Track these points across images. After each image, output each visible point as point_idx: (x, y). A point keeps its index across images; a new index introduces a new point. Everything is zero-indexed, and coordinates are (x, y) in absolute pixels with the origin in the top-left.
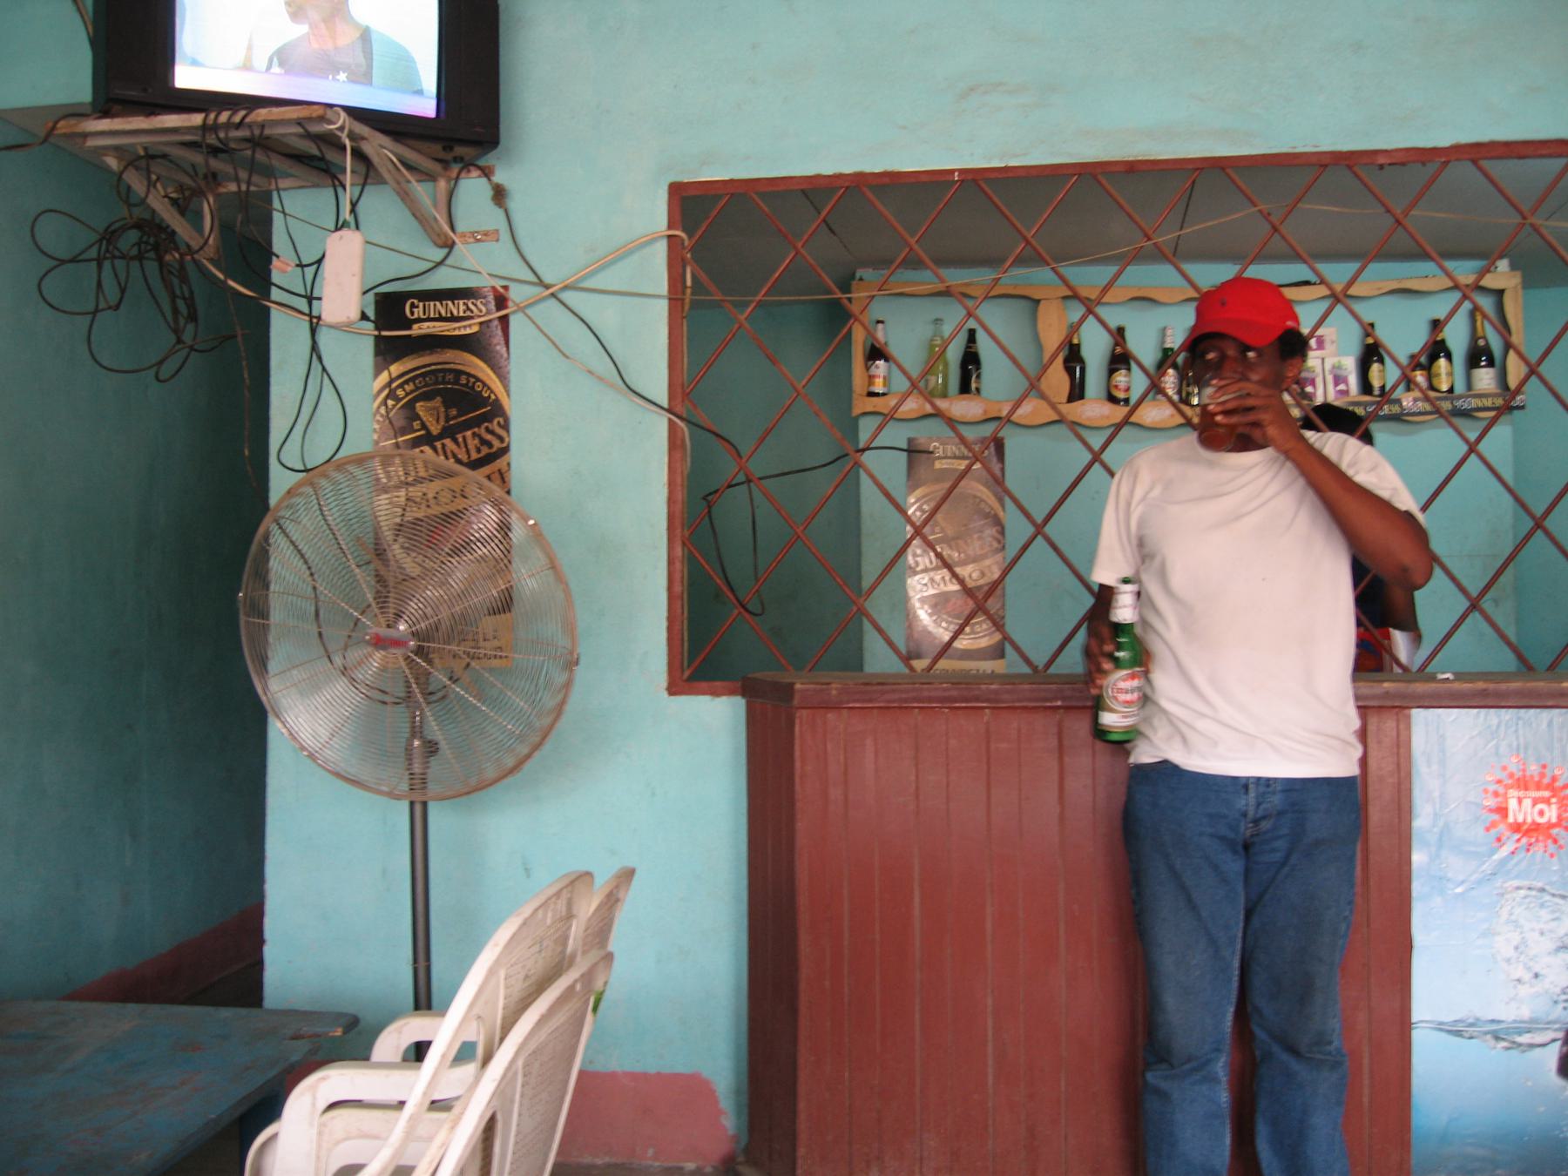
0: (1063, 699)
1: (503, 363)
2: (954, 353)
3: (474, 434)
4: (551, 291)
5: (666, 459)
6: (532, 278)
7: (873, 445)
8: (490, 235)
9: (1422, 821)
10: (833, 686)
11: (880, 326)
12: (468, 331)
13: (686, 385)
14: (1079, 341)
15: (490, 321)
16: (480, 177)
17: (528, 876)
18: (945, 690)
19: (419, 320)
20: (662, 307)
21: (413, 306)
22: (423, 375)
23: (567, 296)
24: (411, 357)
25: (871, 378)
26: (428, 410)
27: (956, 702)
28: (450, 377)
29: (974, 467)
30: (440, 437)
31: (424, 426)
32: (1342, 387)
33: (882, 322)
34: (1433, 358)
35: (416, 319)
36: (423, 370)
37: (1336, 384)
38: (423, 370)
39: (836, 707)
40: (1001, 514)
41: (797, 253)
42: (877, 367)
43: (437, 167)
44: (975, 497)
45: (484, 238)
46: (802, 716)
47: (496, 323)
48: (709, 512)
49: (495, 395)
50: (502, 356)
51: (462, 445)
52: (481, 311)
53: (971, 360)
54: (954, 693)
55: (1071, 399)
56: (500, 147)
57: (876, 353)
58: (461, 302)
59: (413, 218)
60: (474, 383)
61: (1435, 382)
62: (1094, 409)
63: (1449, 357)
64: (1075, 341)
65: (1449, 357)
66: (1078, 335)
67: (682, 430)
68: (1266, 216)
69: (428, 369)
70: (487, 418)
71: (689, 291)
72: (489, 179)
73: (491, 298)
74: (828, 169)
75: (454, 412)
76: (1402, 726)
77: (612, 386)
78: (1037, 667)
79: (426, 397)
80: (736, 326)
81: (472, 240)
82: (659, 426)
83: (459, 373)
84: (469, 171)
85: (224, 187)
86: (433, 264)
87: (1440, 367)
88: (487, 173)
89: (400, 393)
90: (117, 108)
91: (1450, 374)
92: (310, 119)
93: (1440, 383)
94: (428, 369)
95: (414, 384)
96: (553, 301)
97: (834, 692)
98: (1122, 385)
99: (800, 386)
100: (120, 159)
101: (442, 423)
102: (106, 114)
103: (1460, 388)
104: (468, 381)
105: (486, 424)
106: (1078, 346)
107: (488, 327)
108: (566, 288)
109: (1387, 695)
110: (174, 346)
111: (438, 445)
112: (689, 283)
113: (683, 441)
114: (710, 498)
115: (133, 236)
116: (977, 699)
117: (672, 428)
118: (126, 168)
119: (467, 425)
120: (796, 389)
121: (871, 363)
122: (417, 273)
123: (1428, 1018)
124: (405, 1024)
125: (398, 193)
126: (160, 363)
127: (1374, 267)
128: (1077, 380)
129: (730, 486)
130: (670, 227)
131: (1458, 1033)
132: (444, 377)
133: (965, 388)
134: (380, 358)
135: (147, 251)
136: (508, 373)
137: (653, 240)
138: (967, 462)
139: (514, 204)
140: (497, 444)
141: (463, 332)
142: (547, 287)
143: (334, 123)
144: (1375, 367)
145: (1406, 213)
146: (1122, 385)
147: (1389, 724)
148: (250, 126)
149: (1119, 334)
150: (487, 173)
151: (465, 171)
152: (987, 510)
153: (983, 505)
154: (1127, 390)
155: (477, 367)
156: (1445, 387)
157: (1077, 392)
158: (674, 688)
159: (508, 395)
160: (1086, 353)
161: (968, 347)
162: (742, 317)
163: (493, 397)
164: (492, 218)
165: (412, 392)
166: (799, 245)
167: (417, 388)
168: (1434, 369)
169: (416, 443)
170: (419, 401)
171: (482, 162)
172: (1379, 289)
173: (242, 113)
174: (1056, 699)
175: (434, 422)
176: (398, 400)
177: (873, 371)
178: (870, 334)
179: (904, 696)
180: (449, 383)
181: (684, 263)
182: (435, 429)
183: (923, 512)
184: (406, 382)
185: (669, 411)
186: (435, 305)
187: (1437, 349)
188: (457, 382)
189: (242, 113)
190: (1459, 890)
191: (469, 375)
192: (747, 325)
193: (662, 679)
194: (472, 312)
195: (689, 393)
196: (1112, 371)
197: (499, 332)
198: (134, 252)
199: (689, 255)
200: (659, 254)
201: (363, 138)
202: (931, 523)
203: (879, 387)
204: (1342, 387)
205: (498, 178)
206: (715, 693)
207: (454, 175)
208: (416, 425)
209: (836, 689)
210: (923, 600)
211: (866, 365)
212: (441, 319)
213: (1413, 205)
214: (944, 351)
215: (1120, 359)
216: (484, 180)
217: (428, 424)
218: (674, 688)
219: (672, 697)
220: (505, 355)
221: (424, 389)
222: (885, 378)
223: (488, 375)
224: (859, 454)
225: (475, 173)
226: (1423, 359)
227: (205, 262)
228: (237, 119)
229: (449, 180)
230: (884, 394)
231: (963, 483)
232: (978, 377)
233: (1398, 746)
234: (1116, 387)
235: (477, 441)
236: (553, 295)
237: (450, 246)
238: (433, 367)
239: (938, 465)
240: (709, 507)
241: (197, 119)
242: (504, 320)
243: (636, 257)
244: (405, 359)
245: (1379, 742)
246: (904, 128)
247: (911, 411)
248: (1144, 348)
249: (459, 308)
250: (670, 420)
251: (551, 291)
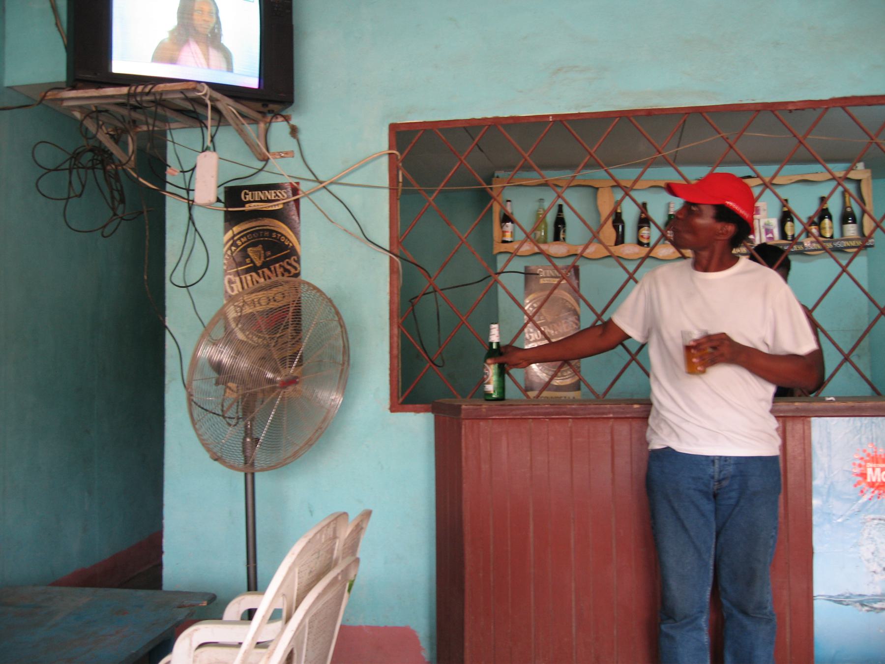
0: (613, 413)
1: (297, 226)
2: (551, 218)
3: (281, 266)
4: (323, 185)
5: (388, 279)
6: (313, 178)
7: (505, 271)
8: (289, 154)
9: (818, 481)
10: (484, 406)
11: (509, 203)
12: (277, 208)
13: (399, 237)
14: (621, 210)
15: (289, 202)
16: (283, 121)
17: (312, 515)
18: (547, 408)
19: (249, 202)
20: (386, 193)
21: (246, 194)
22: (252, 233)
23: (333, 188)
24: (246, 222)
25: (504, 232)
26: (254, 252)
27: (553, 415)
28: (267, 234)
29: (562, 282)
30: (262, 267)
31: (252, 261)
32: (770, 235)
34: (821, 219)
35: (247, 201)
36: (252, 230)
37: (767, 233)
38: (252, 230)
39: (485, 419)
40: (578, 309)
41: (461, 163)
42: (507, 226)
43: (259, 116)
44: (563, 299)
45: (286, 155)
46: (466, 424)
47: (292, 203)
48: (413, 310)
49: (292, 244)
50: (295, 222)
51: (274, 272)
52: (284, 196)
53: (560, 222)
54: (552, 410)
55: (617, 244)
56: (294, 104)
57: (506, 218)
58: (273, 191)
59: (246, 145)
60: (280, 237)
61: (823, 232)
62: (629, 249)
64: (619, 211)
66: (621, 208)
67: (397, 263)
68: (726, 139)
69: (254, 229)
70: (288, 256)
71: (401, 184)
72: (288, 123)
73: (289, 189)
74: (478, 115)
75: (269, 253)
76: (806, 427)
77: (357, 238)
78: (598, 395)
79: (254, 245)
80: (427, 204)
81: (278, 157)
82: (384, 261)
83: (272, 231)
84: (277, 118)
85: (140, 128)
86: (255, 171)
87: (825, 224)
88: (287, 119)
89: (239, 243)
90: (80, 85)
92: (187, 90)
93: (826, 232)
94: (254, 229)
95: (247, 237)
96: (324, 190)
97: (484, 410)
98: (646, 236)
99: (463, 237)
100: (81, 113)
101: (262, 259)
102: (74, 88)
104: (277, 236)
105: (287, 260)
106: (620, 213)
107: (288, 205)
108: (332, 183)
109: (797, 410)
110: (111, 218)
111: (260, 272)
112: (401, 180)
113: (398, 269)
114: (413, 301)
115: (89, 155)
116: (565, 414)
117: (391, 260)
118: (85, 118)
119: (276, 261)
120: (462, 240)
121: (503, 224)
122: (248, 175)
123: (823, 593)
124: (242, 599)
125: (237, 131)
126: (104, 227)
127: (787, 168)
128: (620, 233)
129: (424, 294)
130: (390, 148)
132: (263, 234)
133: (557, 238)
134: (227, 223)
135: (97, 164)
136: (299, 231)
137: (380, 156)
138: (558, 279)
139: (302, 136)
140: (293, 271)
141: (274, 208)
142: (321, 183)
143: (201, 92)
144: (789, 224)
145: (805, 136)
146: (646, 236)
147: (799, 426)
148: (154, 94)
149: (643, 207)
150: (287, 119)
151: (274, 118)
152: (570, 307)
153: (567, 304)
154: (648, 238)
155: (282, 227)
156: (828, 235)
157: (620, 240)
158: (394, 408)
159: (300, 244)
160: (625, 217)
161: (558, 215)
162: (431, 199)
163: (291, 245)
164: (289, 144)
165: (245, 242)
166: (463, 158)
167: (249, 240)
168: (822, 225)
169: (248, 271)
170: (248, 247)
171: (284, 113)
172: (791, 180)
173: (150, 86)
174: (609, 413)
175: (258, 259)
176: (238, 247)
177: (505, 229)
178: (503, 208)
179: (523, 412)
180: (266, 237)
181: (398, 169)
182: (258, 263)
183: (534, 308)
184: (242, 237)
185: (390, 252)
186: (258, 193)
187: (824, 213)
188: (270, 236)
189: (150, 86)
191: (277, 232)
192: (433, 203)
193: (387, 403)
194: (279, 197)
195: (401, 242)
196: (639, 228)
197: (294, 208)
198: (90, 164)
199: (400, 164)
200: (384, 164)
201: (218, 100)
202: (538, 314)
203: (508, 238)
204: (770, 235)
205: (294, 121)
206: (417, 411)
207: (268, 120)
208: (248, 261)
209: (485, 408)
211: (501, 225)
212: (261, 201)
213: (809, 131)
214: (544, 217)
215: (644, 221)
216: (285, 123)
217: (254, 260)
218: (394, 408)
219: (393, 413)
220: (298, 221)
221: (252, 241)
222: (511, 232)
223: (288, 232)
224: (497, 276)
225: (280, 119)
226: (816, 220)
227: (129, 169)
228: (147, 90)
229: (266, 123)
230: (511, 242)
231: (556, 291)
232: (564, 231)
233: (804, 438)
234: (642, 236)
235: (282, 270)
236: (324, 187)
237: (266, 160)
238: (257, 228)
239: (542, 281)
240: (413, 306)
241: (125, 90)
242: (297, 202)
243: (370, 167)
244: (241, 224)
245: (793, 437)
246: (521, 92)
247: (526, 250)
248: (658, 214)
249: (271, 195)
250: (391, 257)
251: (323, 185)
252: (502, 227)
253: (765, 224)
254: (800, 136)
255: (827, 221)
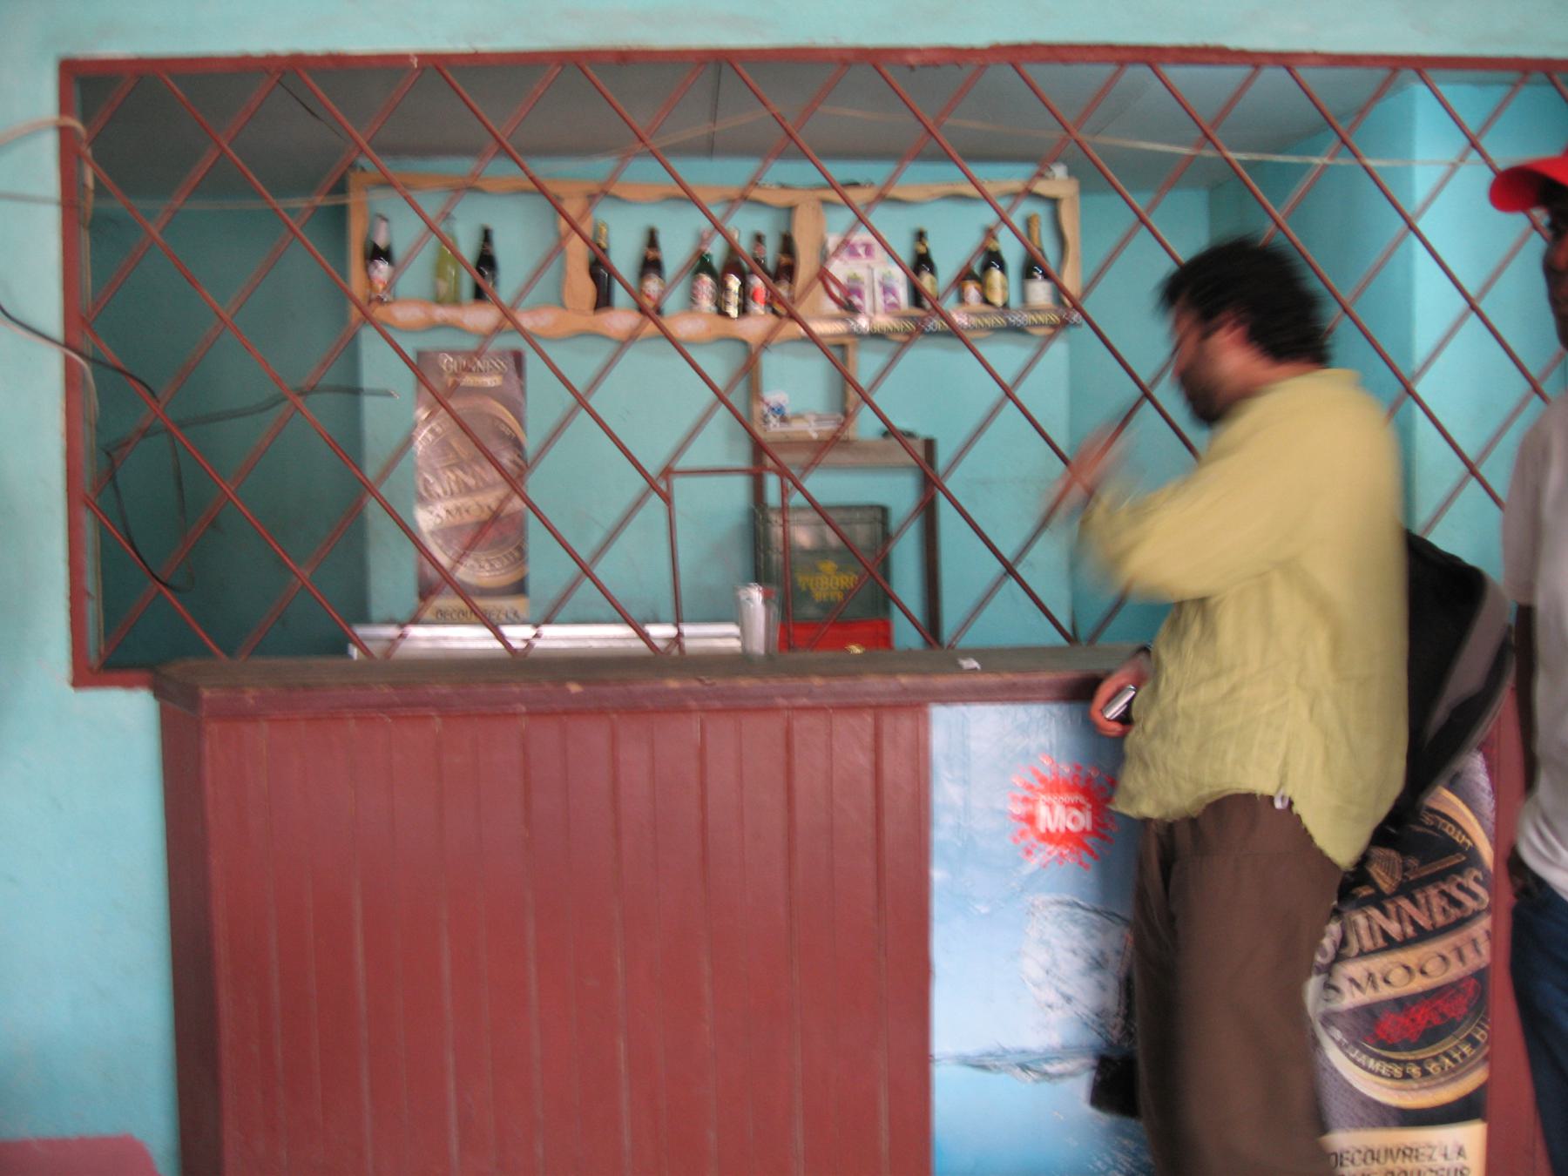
9: (942, 833)
11: (384, 224)
33: (385, 219)
34: (986, 267)
39: (251, 716)
40: (521, 436)
46: (213, 728)
53: (486, 261)
57: (378, 253)
62: (621, 318)
63: (1003, 268)
65: (1003, 268)
91: (1005, 288)
103: (1014, 302)
109: (905, 690)
131: (984, 1067)
133: (479, 294)
147: (906, 723)
149: (652, 240)
153: (503, 428)
157: (603, 301)
190: (984, 910)
204: (892, 299)
206: (128, 685)
210: (432, 533)
215: (650, 265)
226: (976, 269)
248: (675, 254)
252: (366, 268)
253: (884, 277)
254: (930, 122)
255: (996, 274)
